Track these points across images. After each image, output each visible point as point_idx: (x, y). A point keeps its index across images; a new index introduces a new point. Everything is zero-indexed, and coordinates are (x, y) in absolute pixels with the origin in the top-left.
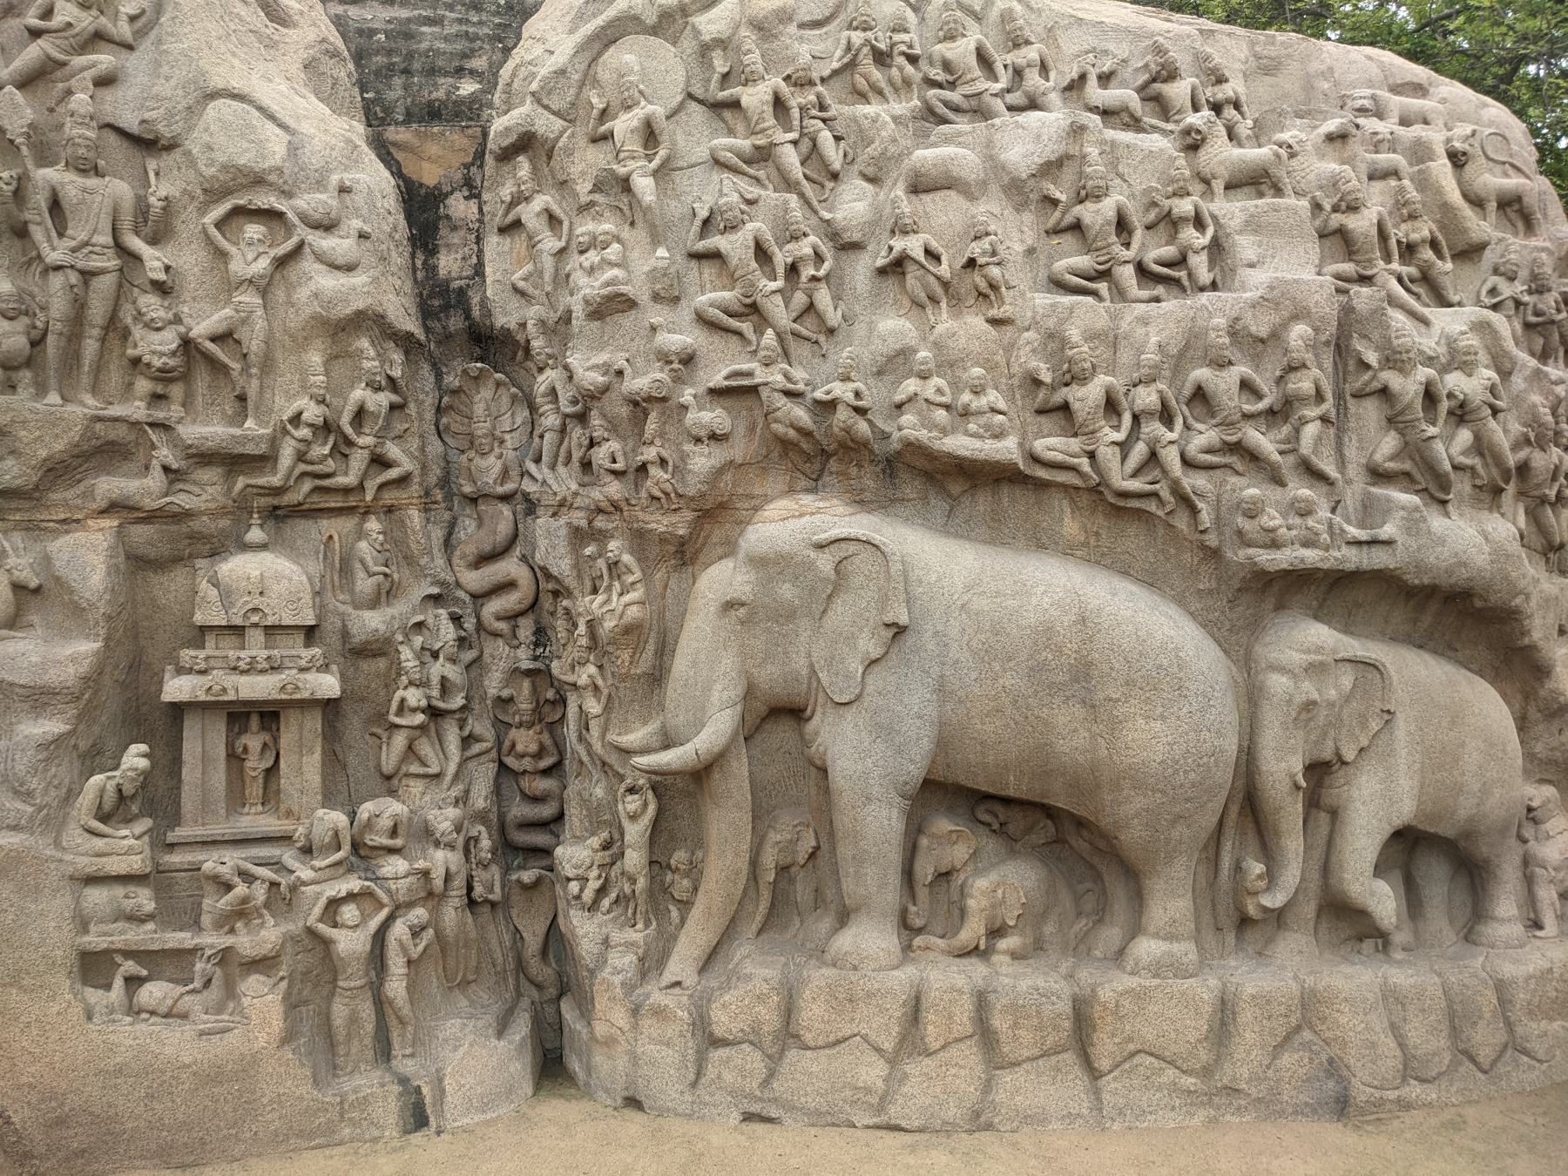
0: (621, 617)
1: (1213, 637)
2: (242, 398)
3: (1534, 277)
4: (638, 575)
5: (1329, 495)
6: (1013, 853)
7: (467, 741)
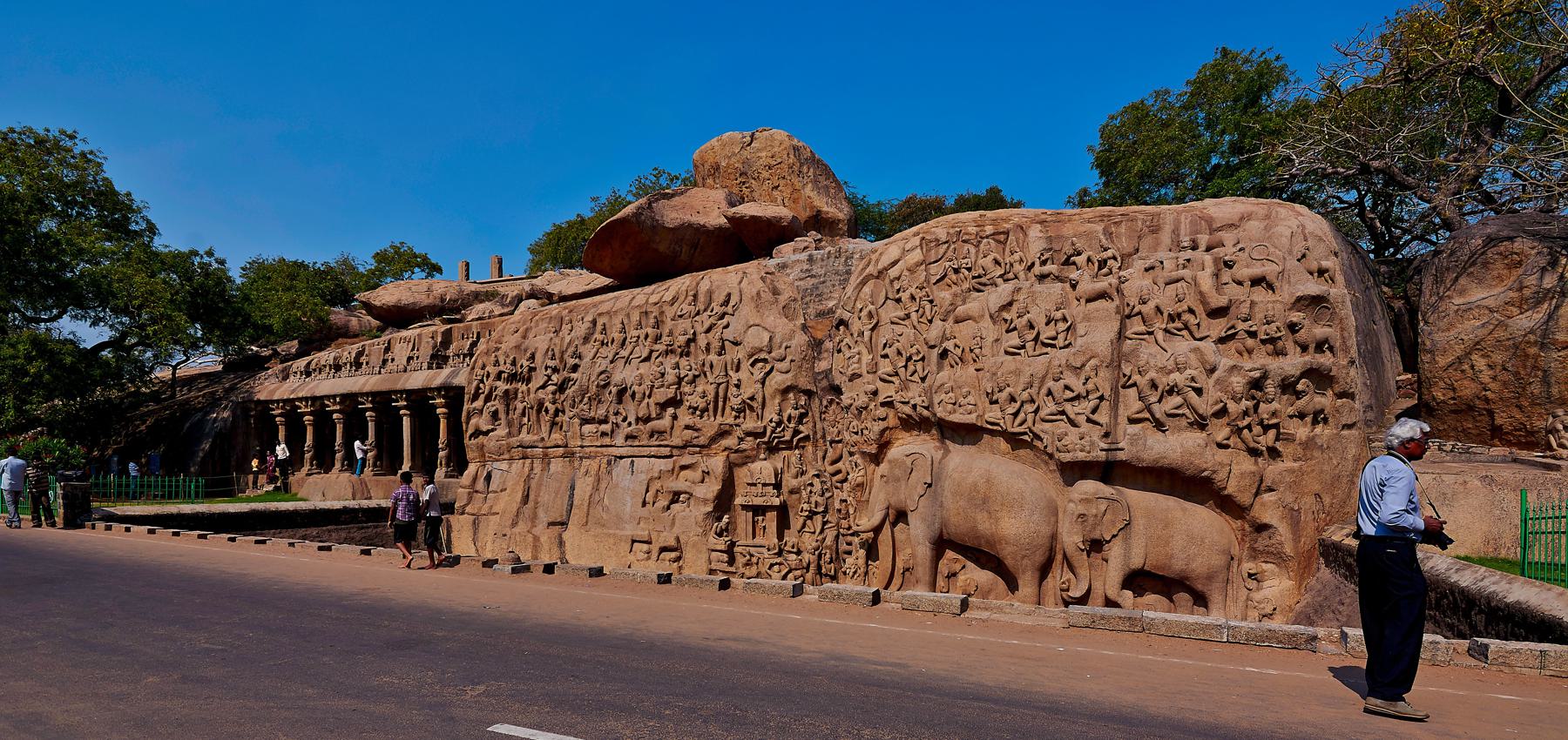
7: (825, 523)
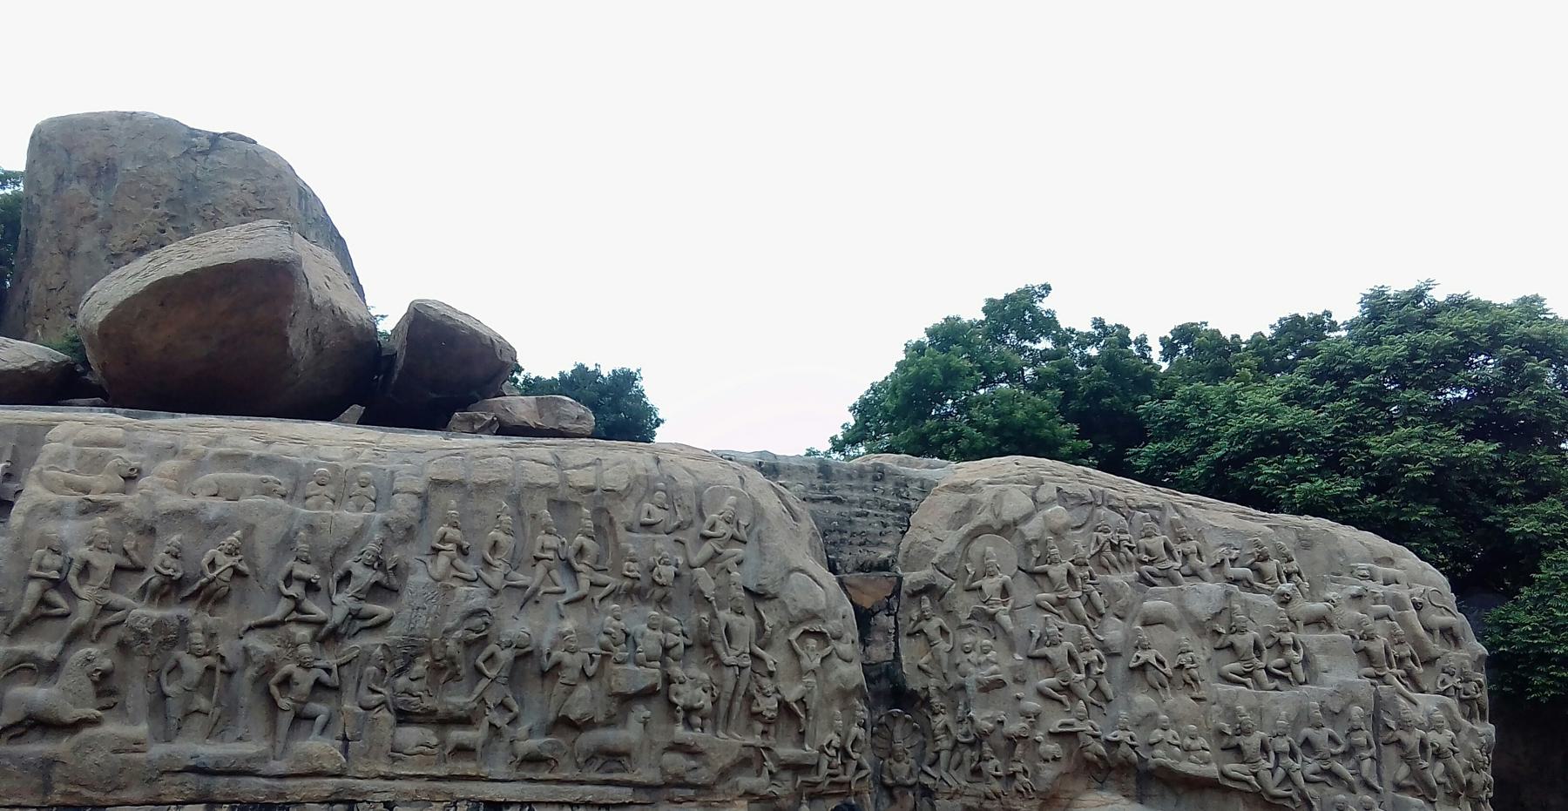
2: (803, 734)
3: (1463, 674)
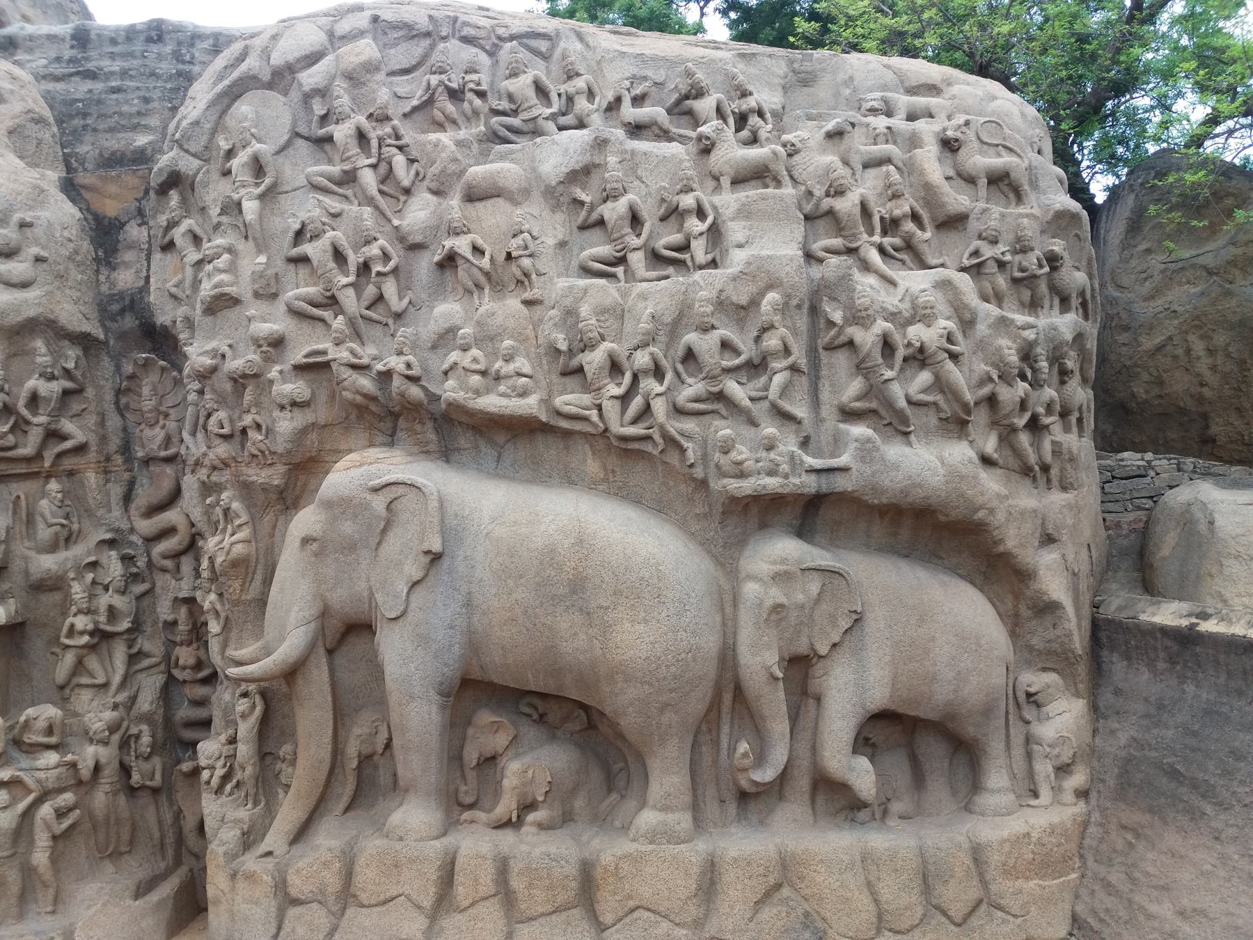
0: (228, 554)
1: (709, 552)
3: (1019, 239)
4: (244, 518)
5: (797, 432)
6: (553, 737)
7: (133, 658)
